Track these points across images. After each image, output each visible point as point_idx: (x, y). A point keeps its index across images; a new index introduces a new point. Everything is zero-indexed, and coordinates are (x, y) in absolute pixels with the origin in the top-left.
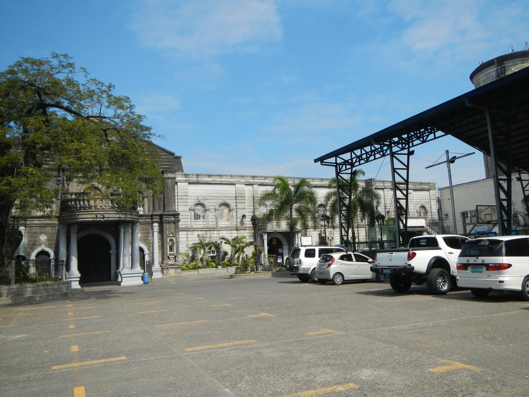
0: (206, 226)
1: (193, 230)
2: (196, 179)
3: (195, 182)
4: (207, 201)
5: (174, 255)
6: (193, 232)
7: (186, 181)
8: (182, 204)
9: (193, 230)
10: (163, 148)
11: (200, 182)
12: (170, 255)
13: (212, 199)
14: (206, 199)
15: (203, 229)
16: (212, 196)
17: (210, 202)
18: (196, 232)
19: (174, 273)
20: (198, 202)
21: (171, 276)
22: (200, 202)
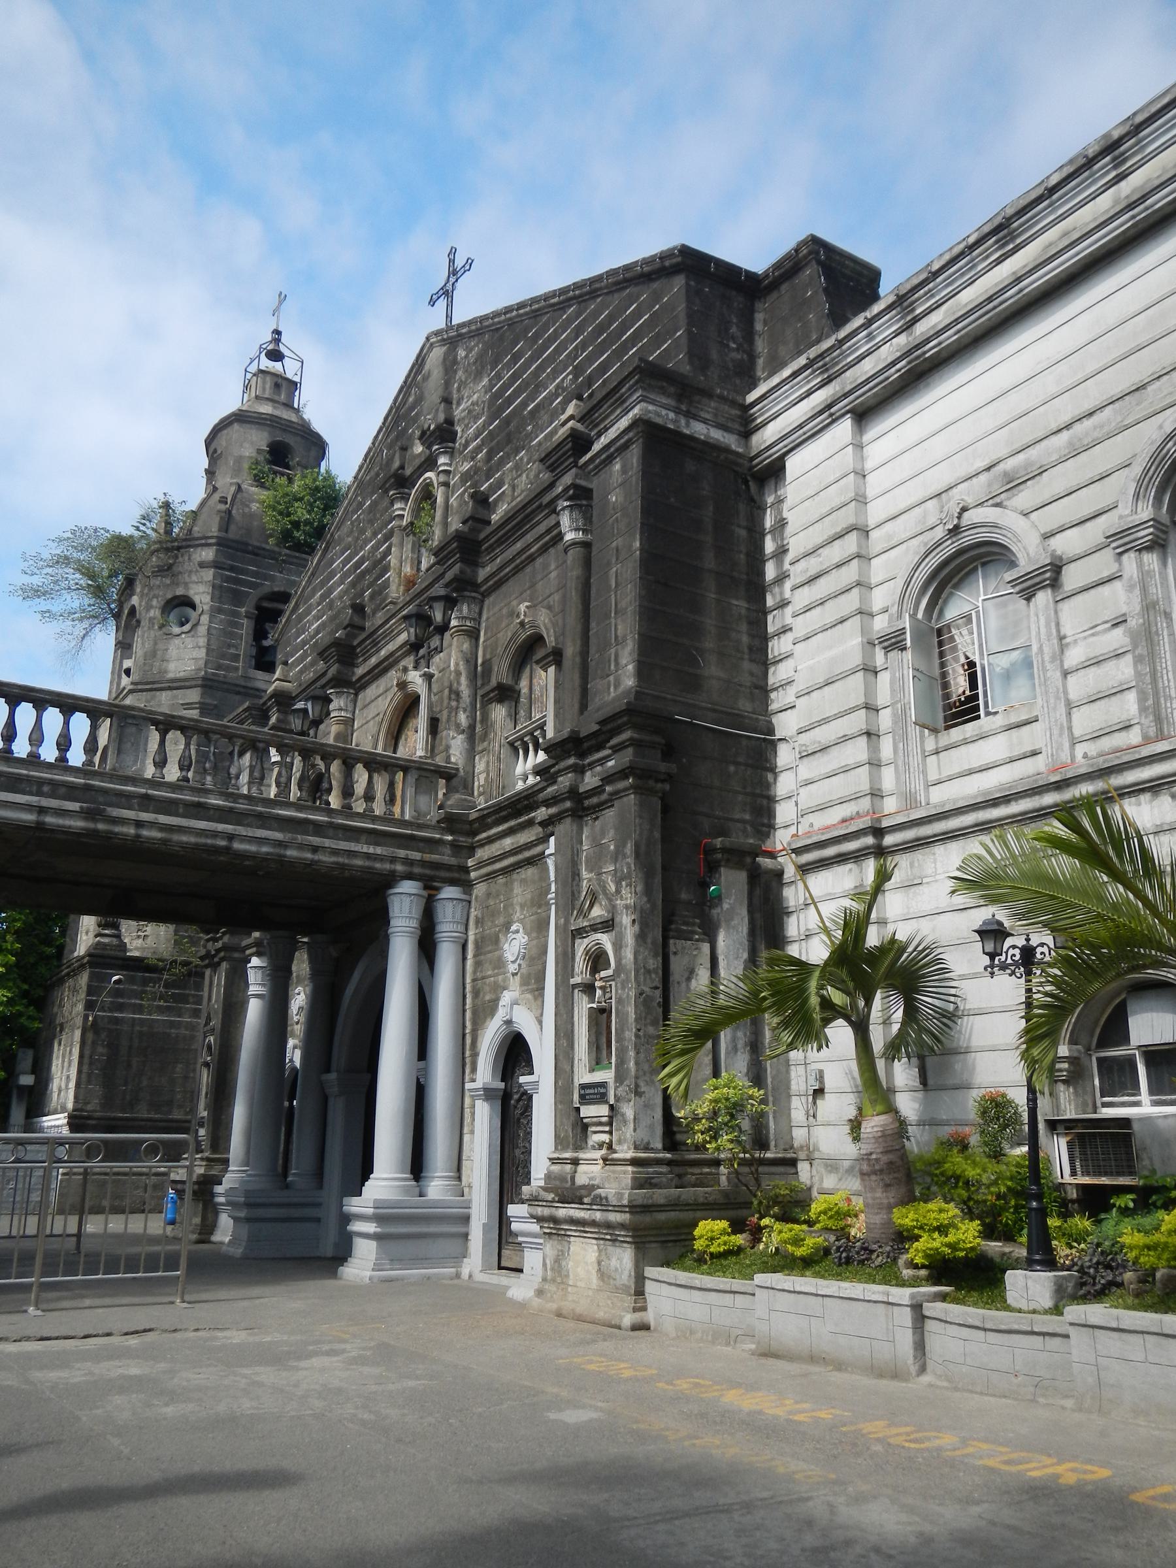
0: (1039, 765)
1: (910, 834)
2: (902, 339)
3: (893, 374)
4: (1025, 498)
5: (602, 1098)
6: (918, 855)
7: (828, 414)
8: (816, 618)
9: (910, 834)
10: (627, 268)
11: (931, 349)
12: (584, 1099)
13: (1075, 452)
14: (1014, 483)
15: (995, 803)
16: (1066, 418)
17: (1059, 488)
18: (939, 850)
19: (595, 1281)
20: (949, 548)
21: (567, 1306)
22: (967, 539)
